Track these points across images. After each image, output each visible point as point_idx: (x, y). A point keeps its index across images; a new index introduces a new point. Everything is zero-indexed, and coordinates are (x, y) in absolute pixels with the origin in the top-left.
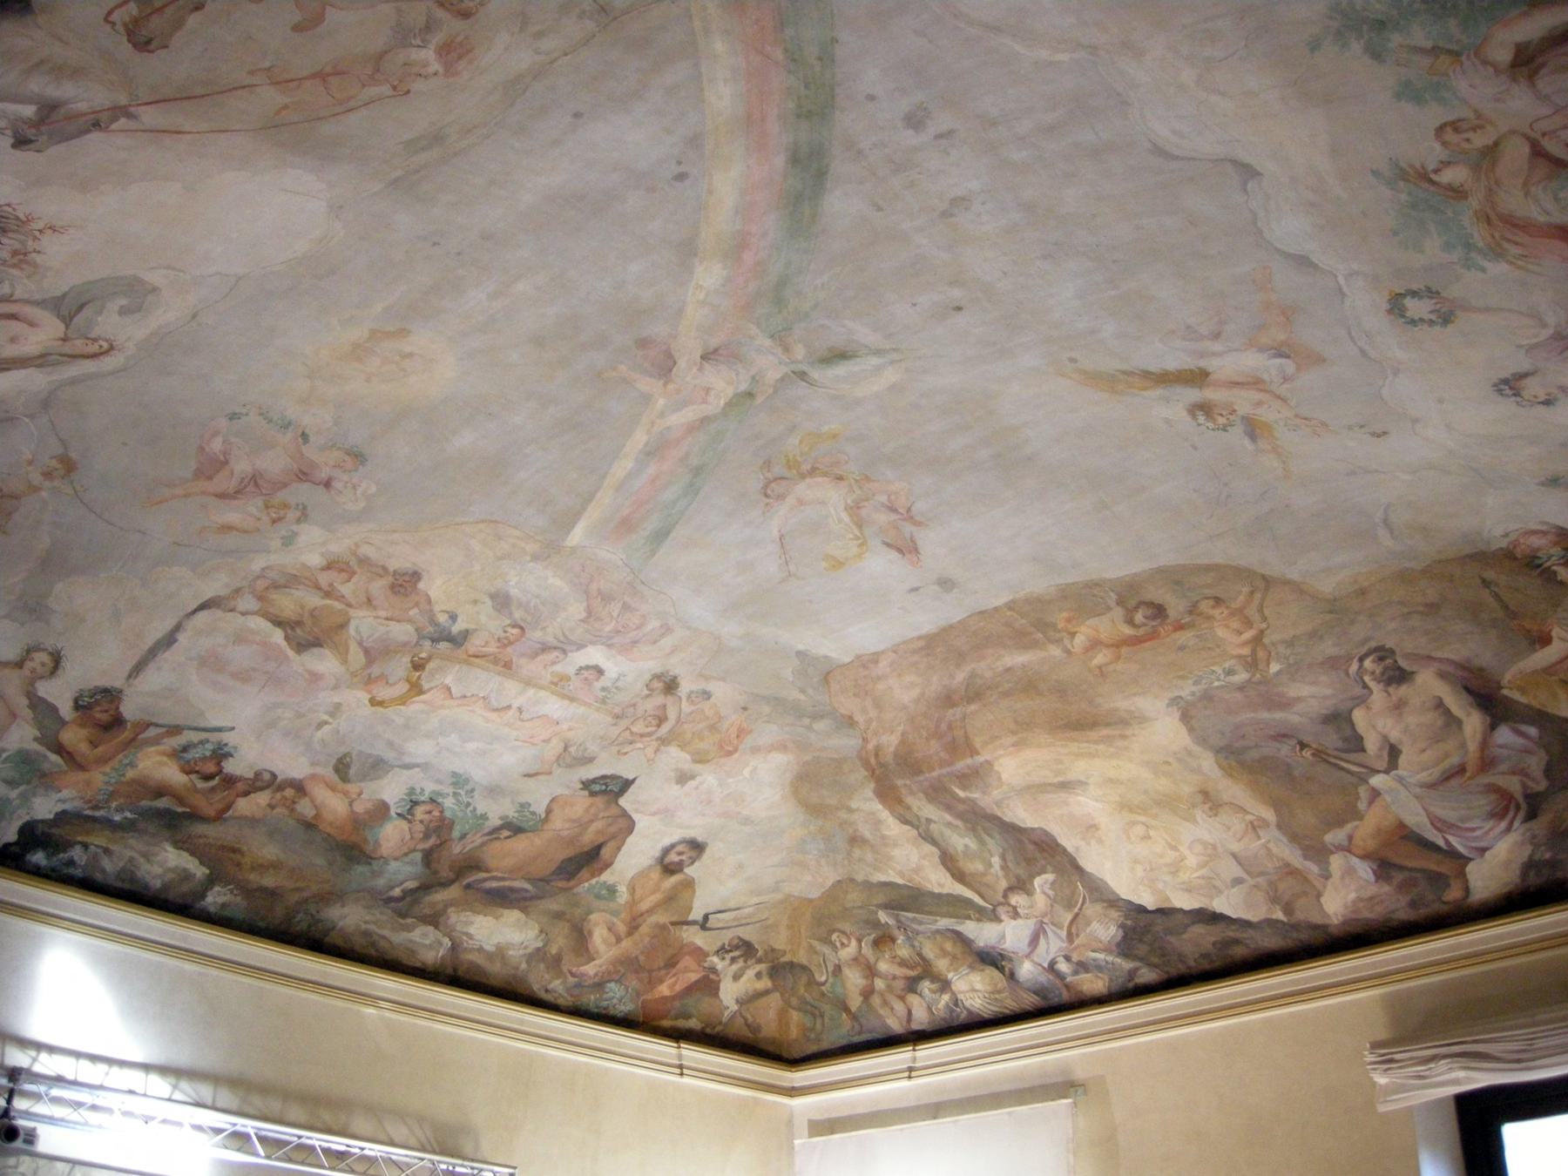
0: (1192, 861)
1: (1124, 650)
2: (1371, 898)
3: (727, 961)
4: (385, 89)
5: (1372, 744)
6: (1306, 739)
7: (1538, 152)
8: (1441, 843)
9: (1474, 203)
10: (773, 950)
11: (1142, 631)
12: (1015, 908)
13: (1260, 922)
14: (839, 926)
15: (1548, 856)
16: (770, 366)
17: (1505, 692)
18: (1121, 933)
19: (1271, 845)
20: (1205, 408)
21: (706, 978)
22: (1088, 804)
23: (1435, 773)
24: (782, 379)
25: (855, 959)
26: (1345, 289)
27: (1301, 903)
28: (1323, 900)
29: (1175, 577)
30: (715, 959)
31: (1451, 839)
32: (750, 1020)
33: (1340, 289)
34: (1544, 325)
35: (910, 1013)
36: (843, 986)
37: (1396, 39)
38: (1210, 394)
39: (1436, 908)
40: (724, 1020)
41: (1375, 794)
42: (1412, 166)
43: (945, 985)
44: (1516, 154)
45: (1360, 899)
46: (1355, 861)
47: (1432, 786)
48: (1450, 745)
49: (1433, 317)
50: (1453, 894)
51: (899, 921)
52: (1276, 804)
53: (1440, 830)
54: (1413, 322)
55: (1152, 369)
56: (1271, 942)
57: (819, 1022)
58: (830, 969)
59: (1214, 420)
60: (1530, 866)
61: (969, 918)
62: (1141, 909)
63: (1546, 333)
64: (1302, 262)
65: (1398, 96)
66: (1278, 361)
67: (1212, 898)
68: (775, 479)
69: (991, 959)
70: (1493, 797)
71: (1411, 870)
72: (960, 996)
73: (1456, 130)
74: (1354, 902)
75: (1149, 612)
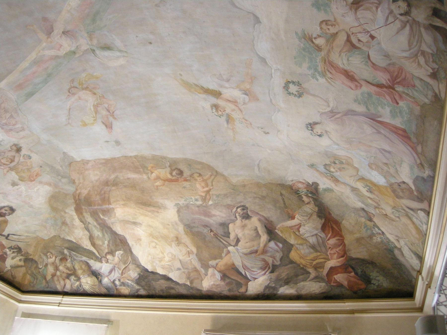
0: (167, 259)
1: (167, 183)
2: (217, 285)
3: (11, 252)
5: (232, 236)
6: (213, 229)
7: (349, 40)
8: (243, 273)
9: (323, 53)
10: (28, 253)
11: (174, 178)
12: (108, 259)
13: (181, 284)
14: (51, 251)
15: (273, 285)
16: (84, 43)
17: (276, 231)
18: (138, 276)
19: (192, 260)
20: (216, 107)
21: (2, 255)
22: (140, 232)
23: (249, 250)
24: (86, 50)
25: (53, 263)
26: (273, 75)
27: (196, 281)
28: (203, 282)
29: (190, 163)
30: (7, 250)
31: (247, 272)
32: (13, 274)
33: (272, 74)
34: (329, 106)
35: (65, 285)
36: (47, 272)
38: (220, 102)
39: (236, 293)
40: (5, 271)
41: (229, 252)
42: (308, 34)
43: (79, 279)
44: (342, 38)
45: (214, 285)
46: (216, 272)
47: (246, 254)
48: (255, 243)
49: (296, 94)
50: (242, 290)
51: (70, 254)
52: (198, 248)
53: (244, 269)
54: (290, 94)
56: (183, 291)
57: (35, 280)
58: (44, 264)
60: (267, 287)
61: (92, 259)
62: (147, 270)
63: (329, 109)
64: (263, 60)
65: (313, 5)
66: (244, 96)
67: (169, 272)
68: (74, 87)
69: (96, 274)
70: (263, 263)
71: (232, 279)
72: (82, 284)
73: (326, 24)
74: (212, 285)
75: (178, 172)
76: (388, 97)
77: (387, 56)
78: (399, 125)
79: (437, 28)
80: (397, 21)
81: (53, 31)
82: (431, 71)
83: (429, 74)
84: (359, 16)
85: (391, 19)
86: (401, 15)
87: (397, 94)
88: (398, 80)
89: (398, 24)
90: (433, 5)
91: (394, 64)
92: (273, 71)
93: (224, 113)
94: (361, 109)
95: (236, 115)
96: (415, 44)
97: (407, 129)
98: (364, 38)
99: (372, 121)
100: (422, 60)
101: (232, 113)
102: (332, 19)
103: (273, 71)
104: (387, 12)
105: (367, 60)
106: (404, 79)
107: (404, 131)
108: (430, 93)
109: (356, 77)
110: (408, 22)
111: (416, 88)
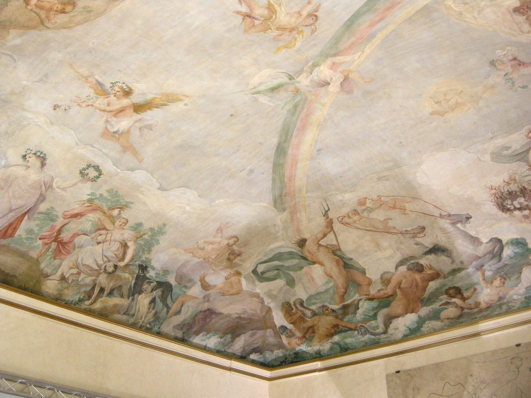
4: (383, 198)
7: (105, 229)
16: (304, 81)
20: (128, 93)
24: (300, 75)
26: (115, 167)
33: (117, 167)
34: (57, 187)
37: (150, 233)
44: (109, 226)
49: (86, 172)
54: (89, 166)
55: (155, 109)
59: (119, 88)
63: (55, 186)
64: (132, 170)
66: (115, 129)
68: (310, 25)
76: (48, 233)
77: (81, 247)
78: (18, 233)
79: (93, 288)
80: (102, 262)
81: (341, 83)
82: (66, 277)
83: (64, 274)
84: (116, 243)
85: (105, 259)
86: (105, 267)
87: (49, 242)
88: (60, 247)
89: (100, 262)
90: (106, 289)
91: (74, 249)
92: (119, 170)
93: (114, 92)
94: (43, 207)
95: (101, 102)
96: (86, 269)
97: (13, 238)
98: (100, 238)
99: (26, 210)
100: (74, 271)
101: (106, 100)
102: (124, 227)
103: (119, 170)
104: (110, 259)
107: (11, 236)
108: (48, 270)
109: (74, 219)
110: (100, 269)
111: (52, 260)
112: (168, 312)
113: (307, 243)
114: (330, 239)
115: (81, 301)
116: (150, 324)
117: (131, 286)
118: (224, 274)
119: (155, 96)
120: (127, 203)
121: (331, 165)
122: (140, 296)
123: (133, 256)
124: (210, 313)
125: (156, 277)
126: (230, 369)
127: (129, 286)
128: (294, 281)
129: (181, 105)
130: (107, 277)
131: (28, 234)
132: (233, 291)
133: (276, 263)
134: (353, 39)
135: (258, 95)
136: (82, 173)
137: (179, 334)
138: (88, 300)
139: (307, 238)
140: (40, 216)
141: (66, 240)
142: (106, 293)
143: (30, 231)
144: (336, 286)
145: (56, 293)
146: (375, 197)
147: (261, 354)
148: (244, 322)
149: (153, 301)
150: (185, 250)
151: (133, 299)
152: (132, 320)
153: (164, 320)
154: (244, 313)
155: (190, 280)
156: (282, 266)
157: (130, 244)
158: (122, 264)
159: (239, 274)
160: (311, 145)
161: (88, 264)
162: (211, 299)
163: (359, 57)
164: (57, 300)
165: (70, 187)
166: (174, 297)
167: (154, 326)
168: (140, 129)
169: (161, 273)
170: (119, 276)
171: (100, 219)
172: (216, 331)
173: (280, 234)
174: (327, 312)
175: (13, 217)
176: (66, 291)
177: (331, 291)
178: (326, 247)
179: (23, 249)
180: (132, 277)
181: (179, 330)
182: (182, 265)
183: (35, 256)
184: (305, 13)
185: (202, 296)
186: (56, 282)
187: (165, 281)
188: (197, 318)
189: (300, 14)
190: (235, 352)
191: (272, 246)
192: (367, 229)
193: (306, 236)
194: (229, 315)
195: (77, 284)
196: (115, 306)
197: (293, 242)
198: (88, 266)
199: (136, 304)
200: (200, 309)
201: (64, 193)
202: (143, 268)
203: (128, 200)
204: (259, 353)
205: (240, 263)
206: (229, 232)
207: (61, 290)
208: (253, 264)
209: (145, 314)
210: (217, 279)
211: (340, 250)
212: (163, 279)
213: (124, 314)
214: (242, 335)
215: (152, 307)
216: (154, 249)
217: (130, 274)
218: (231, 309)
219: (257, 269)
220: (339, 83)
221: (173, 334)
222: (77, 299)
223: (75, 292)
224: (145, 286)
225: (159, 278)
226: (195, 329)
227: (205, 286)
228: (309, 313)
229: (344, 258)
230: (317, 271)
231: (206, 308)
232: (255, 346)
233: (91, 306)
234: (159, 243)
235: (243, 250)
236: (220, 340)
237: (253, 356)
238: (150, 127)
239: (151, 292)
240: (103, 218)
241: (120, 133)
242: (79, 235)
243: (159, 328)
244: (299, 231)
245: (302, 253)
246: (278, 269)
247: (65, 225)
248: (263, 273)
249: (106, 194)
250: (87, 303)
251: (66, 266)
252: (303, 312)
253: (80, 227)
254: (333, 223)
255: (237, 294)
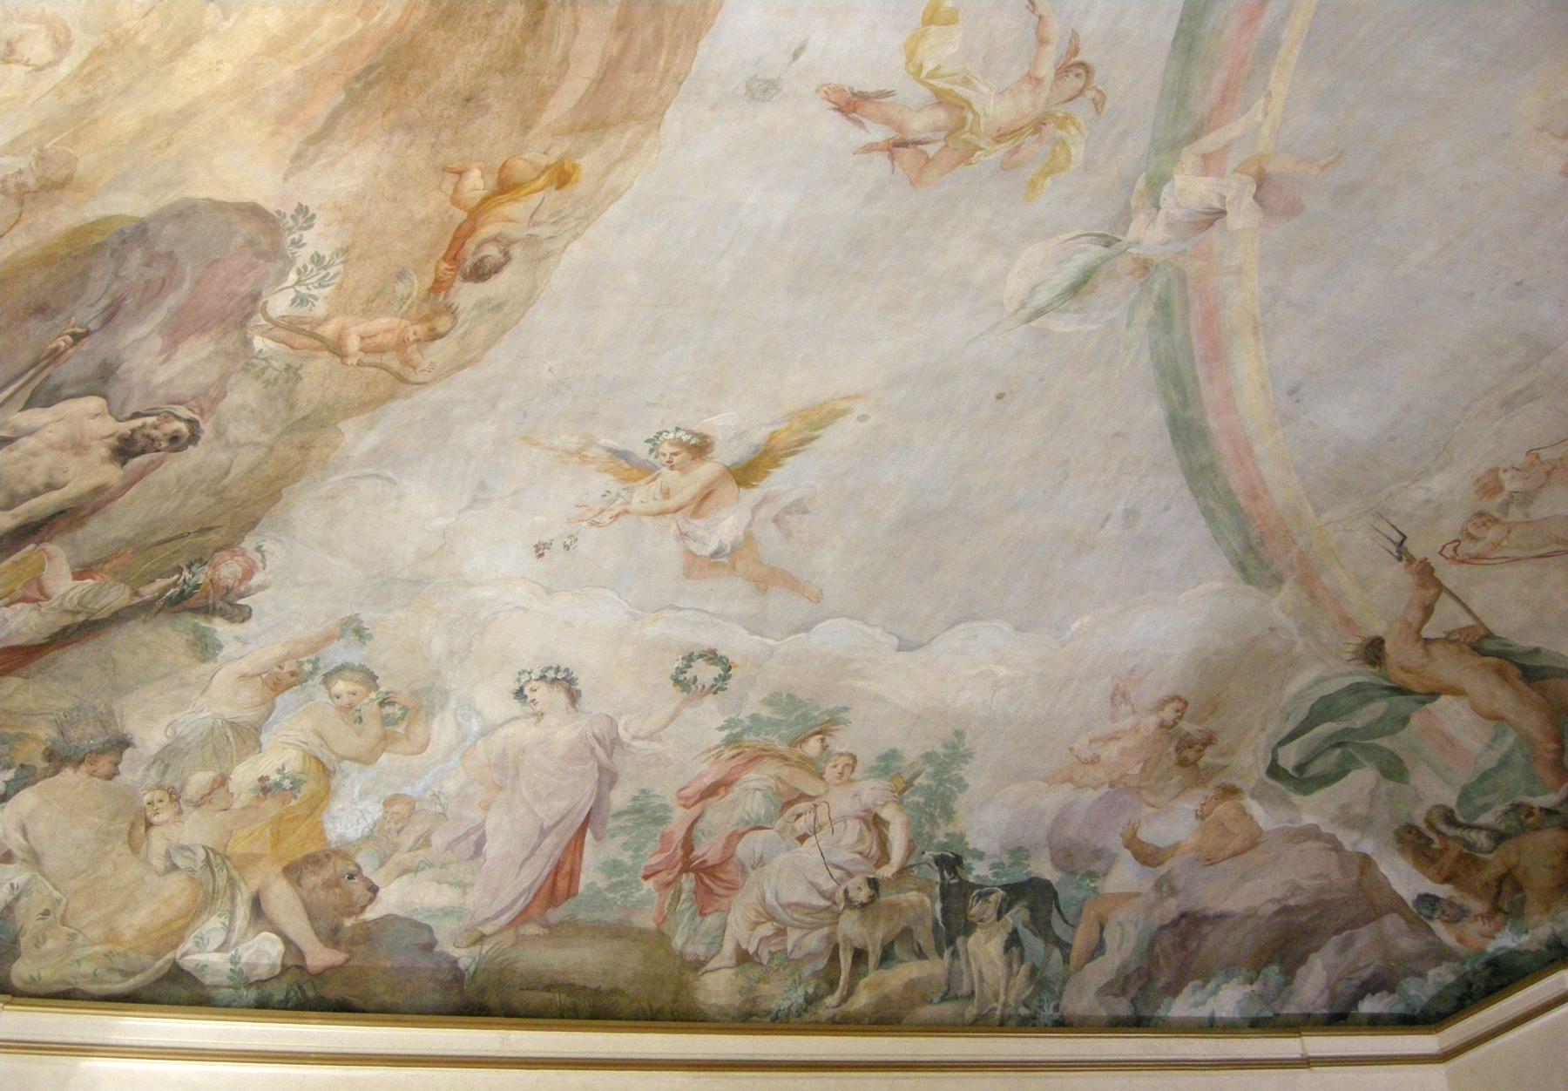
1: (460, 215)
4: (1545, 455)
7: (802, 797)
11: (470, 246)
16: (1149, 235)
24: (1127, 223)
26: (756, 638)
34: (634, 738)
37: (930, 770)
49: (688, 676)
54: (690, 658)
55: (790, 459)
59: (672, 444)
64: (806, 627)
66: (712, 546)
68: (1081, 92)
75: (488, 264)
76: (660, 858)
77: (761, 862)
78: (584, 880)
79: (834, 958)
80: (832, 884)
81: (1255, 197)
82: (751, 950)
84: (850, 823)
85: (837, 873)
86: (846, 892)
88: (707, 881)
89: (828, 885)
90: (870, 949)
91: (743, 870)
92: (771, 642)
93: (664, 459)
94: (619, 798)
95: (644, 495)
98: (801, 826)
99: (582, 819)
100: (767, 929)
101: (655, 487)
103: (771, 642)
104: (852, 868)
105: (752, 825)
106: (710, 892)
107: (571, 892)
108: (698, 949)
109: (710, 800)
111: (698, 919)
112: (1066, 959)
113: (1387, 646)
114: (1448, 616)
115: (811, 1000)
116: (1026, 1005)
117: (936, 923)
118: (1188, 805)
119: (771, 429)
120: (831, 712)
121: (1347, 417)
122: (971, 940)
123: (910, 841)
124: (1190, 924)
125: (996, 874)
126: (1307, 1062)
127: (929, 923)
128: (1401, 761)
129: (849, 424)
130: (863, 918)
131: (610, 876)
132: (1236, 843)
133: (1327, 728)
134: (1221, 76)
135: (1043, 318)
136: (680, 681)
137: (1123, 1008)
138: (832, 991)
139: (1380, 634)
140: (621, 822)
141: (713, 857)
142: (872, 960)
143: (613, 867)
144: (1525, 739)
145: (737, 1000)
146: (1520, 459)
147: (1391, 991)
148: (1304, 918)
149: (1013, 941)
150: (1045, 780)
151: (955, 954)
152: (971, 1011)
153: (1064, 982)
154: (1293, 895)
155: (1098, 854)
156: (1347, 731)
157: (887, 813)
158: (887, 872)
159: (1230, 792)
160: (1263, 387)
161: (795, 900)
162: (1179, 884)
163: (1266, 114)
164: (747, 1019)
165: (665, 726)
166: (1070, 912)
167: (1041, 1007)
168: (776, 520)
169: (1006, 859)
170: (893, 906)
171: (779, 778)
172: (1229, 969)
173: (1299, 648)
174: (1531, 820)
175: (557, 846)
176: (764, 988)
177: (1518, 758)
178: (1448, 640)
179: (612, 917)
180: (930, 897)
181: (1116, 996)
182: (1056, 820)
183: (650, 924)
184: (1046, 70)
185: (1147, 886)
186: (729, 972)
187: (1025, 878)
188: (1157, 949)
189: (1033, 79)
190: (1310, 1010)
191: (1292, 688)
192: (1544, 551)
193: (1377, 628)
194: (1251, 914)
195: (786, 960)
196: (911, 985)
197: (1348, 656)
198: (797, 904)
199: (968, 963)
200: (1157, 923)
201: (658, 746)
202: (951, 863)
203: (832, 706)
204: (1385, 993)
205: (1219, 761)
206: (1151, 693)
207: (751, 990)
208: (1260, 754)
209: (1003, 983)
210: (1175, 823)
211: (1489, 635)
212: (1019, 876)
213: (943, 999)
214: (1313, 956)
215: (1015, 959)
216: (960, 804)
217: (919, 890)
218: (1249, 893)
219: (1281, 763)
220: (1248, 200)
221: (1103, 1013)
222: (801, 1000)
223: (789, 983)
224: (975, 909)
225: (1006, 875)
226: (1162, 981)
227: (1148, 856)
228: (1481, 839)
229: (1512, 653)
230: (1451, 714)
231: (1175, 914)
232: (1366, 974)
233: (844, 1007)
234: (967, 786)
235: (1212, 724)
236: (1248, 988)
237: (1368, 1006)
238: (799, 507)
239: (999, 918)
240: (785, 772)
241: (728, 550)
242: (743, 834)
243: (1056, 1008)
244: (1348, 622)
245: (1387, 679)
246: (1339, 745)
247: (696, 821)
248: (1300, 768)
249: (766, 712)
250: (831, 1000)
251: (739, 923)
252: (1463, 839)
253: (737, 814)
254: (1432, 569)
255: (1253, 845)
